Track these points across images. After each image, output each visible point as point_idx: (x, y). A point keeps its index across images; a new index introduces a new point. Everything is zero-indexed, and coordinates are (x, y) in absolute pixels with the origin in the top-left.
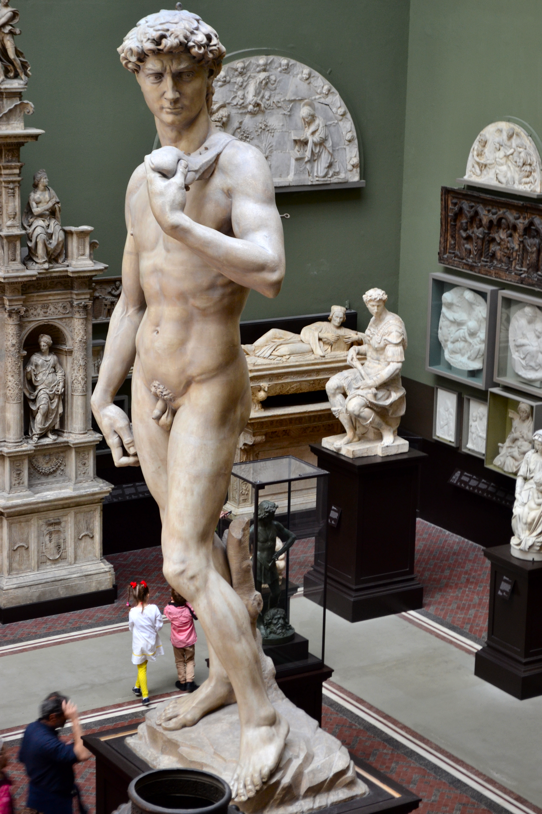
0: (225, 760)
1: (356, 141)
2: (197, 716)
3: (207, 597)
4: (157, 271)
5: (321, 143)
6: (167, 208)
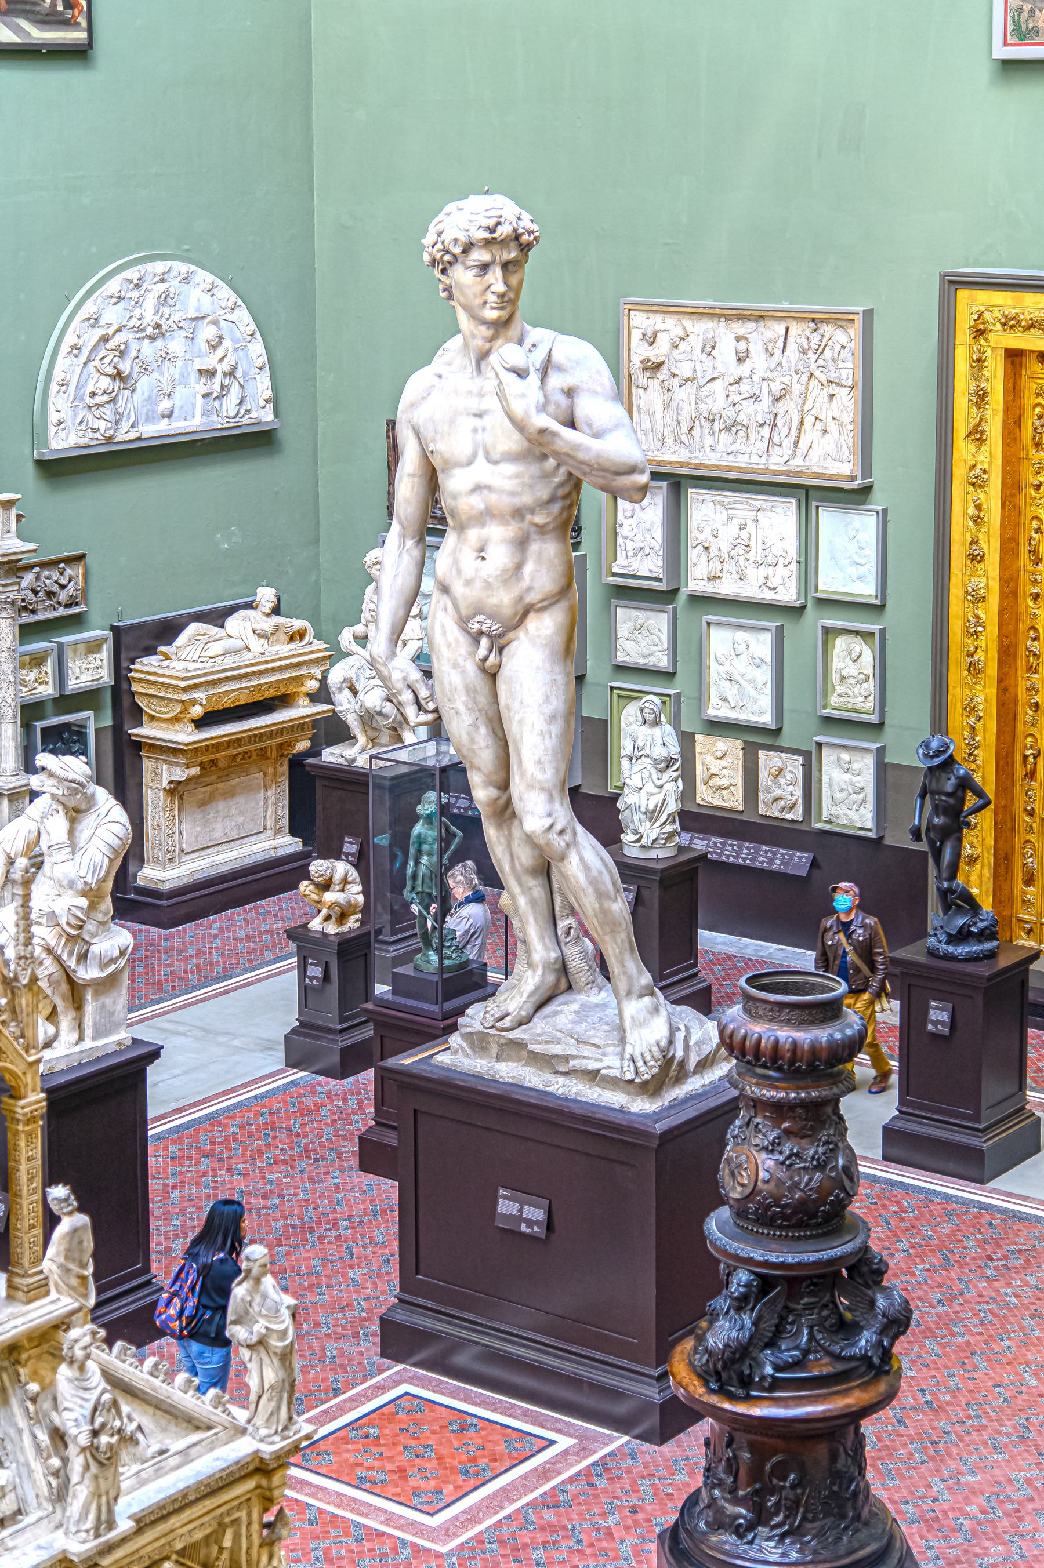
0: (597, 1046)
1: (267, 368)
2: (531, 1011)
3: (579, 853)
4: (477, 488)
5: (231, 374)
6: (533, 410)
